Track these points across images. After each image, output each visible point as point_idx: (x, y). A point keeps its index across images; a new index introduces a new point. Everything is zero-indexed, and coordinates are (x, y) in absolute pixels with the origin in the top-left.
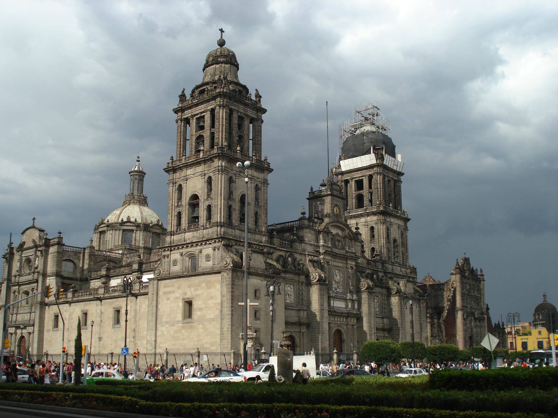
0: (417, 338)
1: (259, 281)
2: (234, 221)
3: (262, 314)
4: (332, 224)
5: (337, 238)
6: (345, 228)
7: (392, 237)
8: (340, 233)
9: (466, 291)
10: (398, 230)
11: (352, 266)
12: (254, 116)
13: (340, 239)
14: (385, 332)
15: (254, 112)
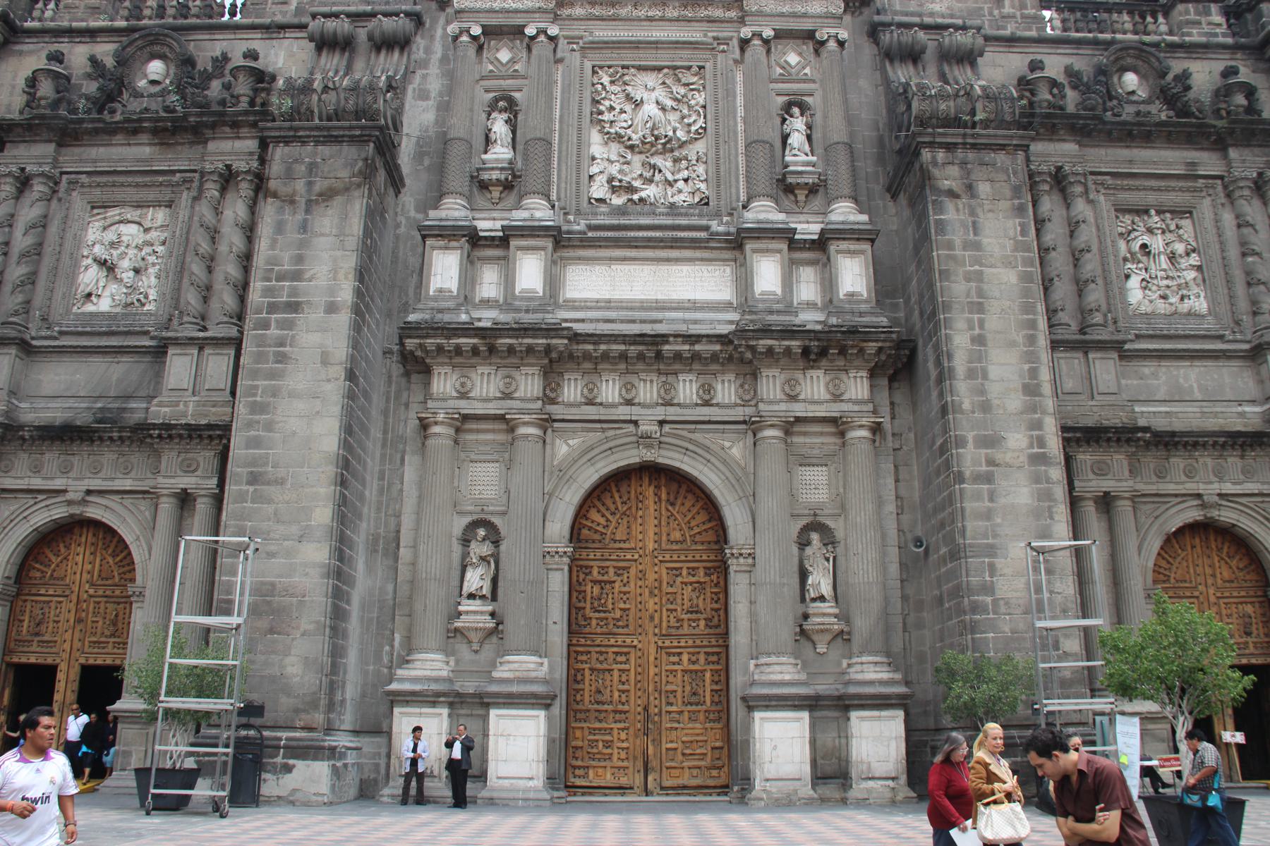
11: (807, 25)
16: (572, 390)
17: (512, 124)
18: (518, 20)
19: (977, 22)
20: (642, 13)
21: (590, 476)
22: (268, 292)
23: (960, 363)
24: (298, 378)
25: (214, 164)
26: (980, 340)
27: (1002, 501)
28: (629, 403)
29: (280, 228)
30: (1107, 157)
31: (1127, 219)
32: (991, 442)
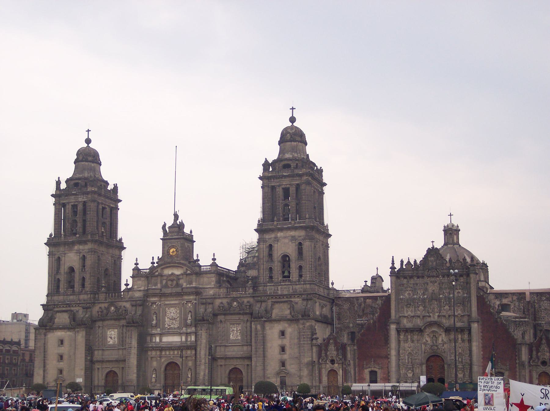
0: (293, 364)
1: (63, 333)
2: (60, 290)
3: (65, 357)
4: (163, 267)
5: (169, 278)
6: (181, 266)
7: (278, 254)
8: (178, 272)
9: (424, 294)
10: (290, 243)
11: (191, 300)
12: (85, 200)
13: (175, 278)
14: (246, 360)
15: (85, 196)
16: (163, 353)
17: (156, 317)
18: (155, 302)
19: (214, 297)
20: (171, 299)
21: (166, 363)
22: (128, 346)
23: (198, 352)
24: (132, 356)
25: (121, 324)
26: (200, 349)
27: (201, 368)
28: (170, 354)
29: (128, 338)
30: (228, 317)
31: (231, 326)
32: (200, 361)
